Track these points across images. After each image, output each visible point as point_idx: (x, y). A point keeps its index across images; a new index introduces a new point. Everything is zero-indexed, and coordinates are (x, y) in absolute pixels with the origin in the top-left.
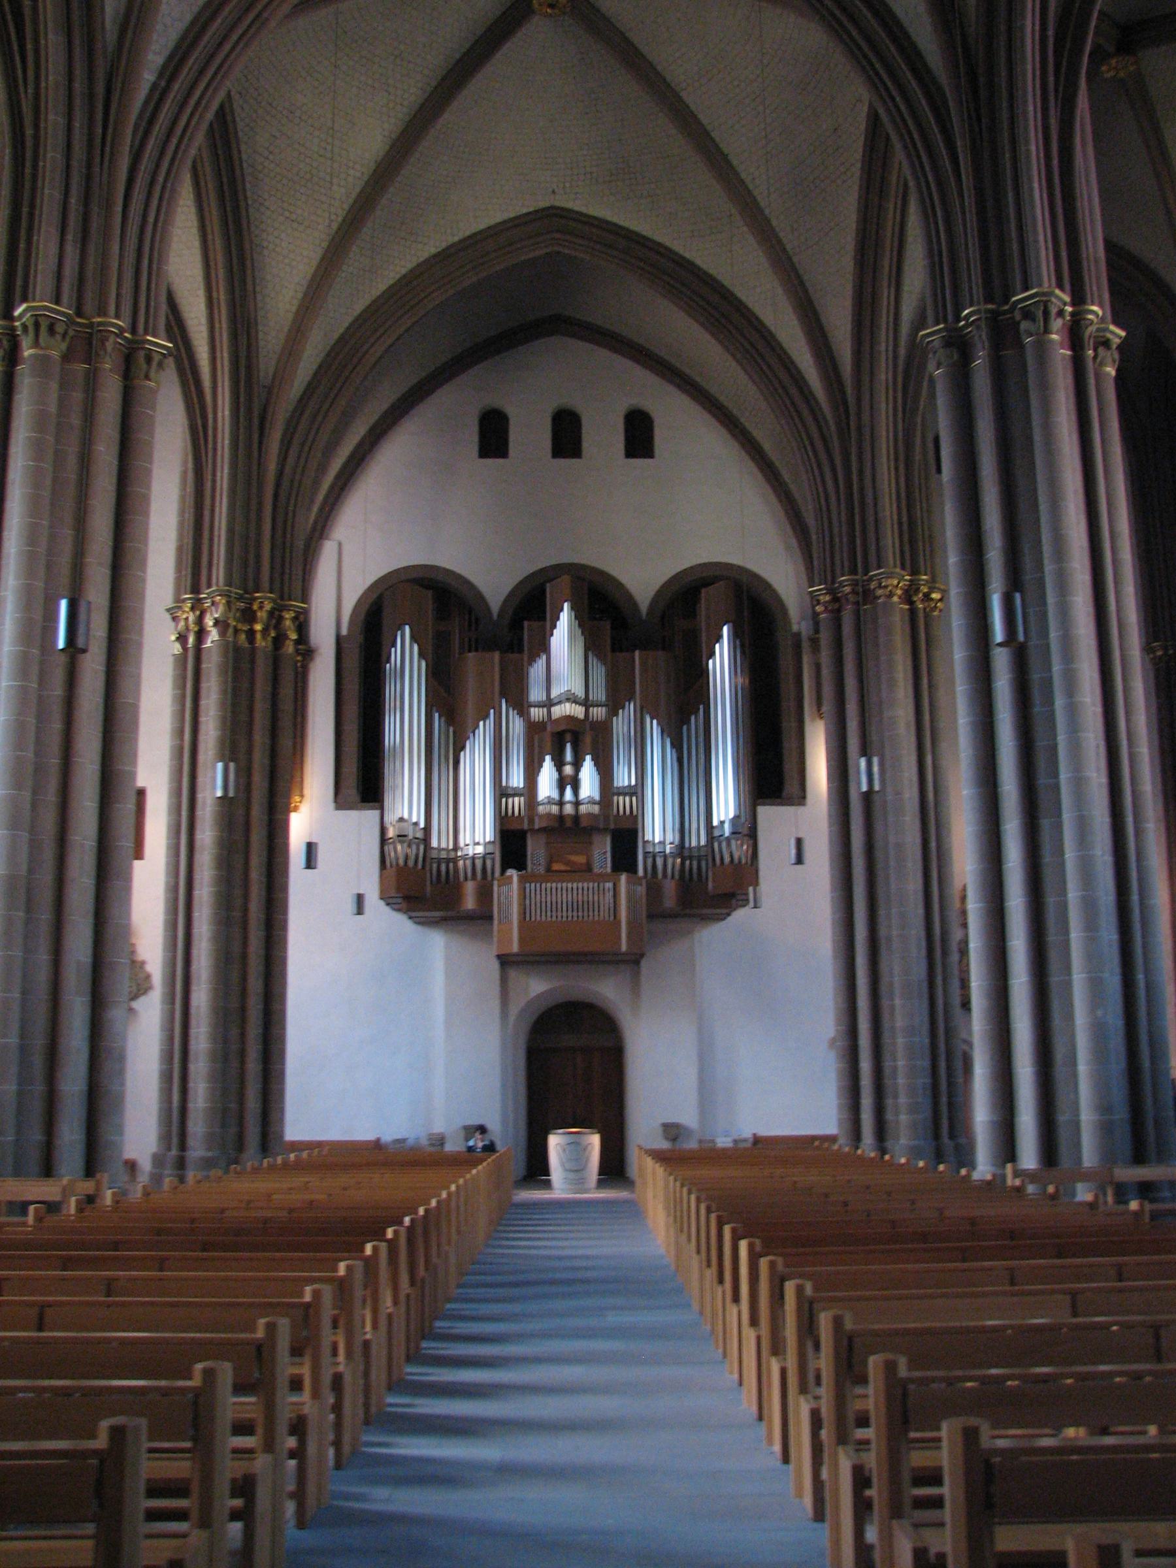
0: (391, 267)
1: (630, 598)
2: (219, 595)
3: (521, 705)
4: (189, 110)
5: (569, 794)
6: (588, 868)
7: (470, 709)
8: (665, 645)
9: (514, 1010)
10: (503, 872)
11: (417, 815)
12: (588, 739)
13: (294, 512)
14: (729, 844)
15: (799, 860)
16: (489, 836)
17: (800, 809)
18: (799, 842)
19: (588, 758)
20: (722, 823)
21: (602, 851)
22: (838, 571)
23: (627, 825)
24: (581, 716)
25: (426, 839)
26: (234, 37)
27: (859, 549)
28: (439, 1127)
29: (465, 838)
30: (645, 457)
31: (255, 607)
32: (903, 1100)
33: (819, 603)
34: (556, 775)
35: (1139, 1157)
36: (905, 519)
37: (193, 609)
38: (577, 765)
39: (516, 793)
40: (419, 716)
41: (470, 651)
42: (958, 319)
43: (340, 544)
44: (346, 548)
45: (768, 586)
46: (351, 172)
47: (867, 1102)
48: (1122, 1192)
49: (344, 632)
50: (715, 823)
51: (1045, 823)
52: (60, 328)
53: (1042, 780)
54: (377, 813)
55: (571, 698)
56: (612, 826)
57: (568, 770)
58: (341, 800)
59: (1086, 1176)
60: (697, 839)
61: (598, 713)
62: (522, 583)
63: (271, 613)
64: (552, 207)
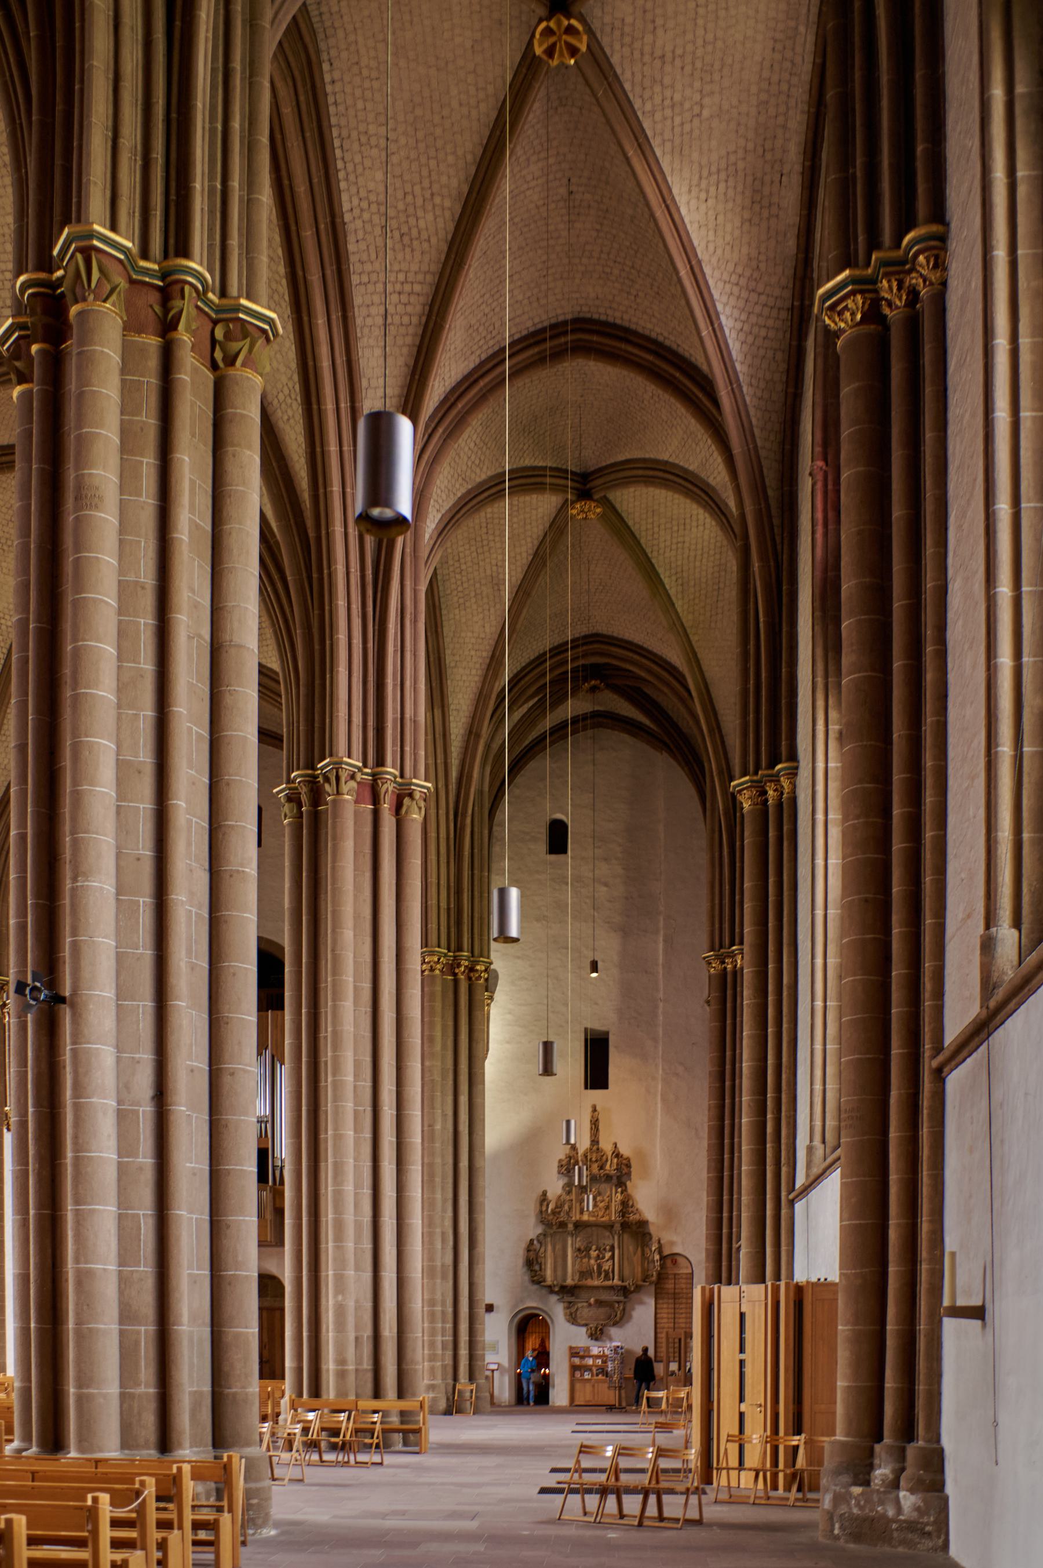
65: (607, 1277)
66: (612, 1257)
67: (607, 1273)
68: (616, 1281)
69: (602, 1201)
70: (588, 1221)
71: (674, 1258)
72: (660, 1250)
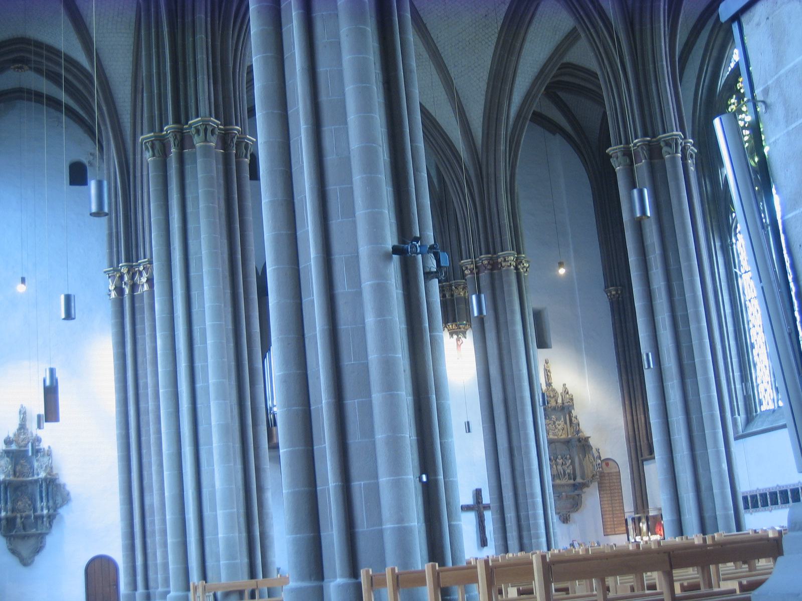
2: (148, 264)
33: (467, 268)
36: (512, 224)
37: (128, 272)
65: (570, 479)
66: (573, 463)
67: (569, 475)
68: (579, 480)
69: (559, 425)
70: (553, 439)
71: (607, 461)
72: (600, 458)
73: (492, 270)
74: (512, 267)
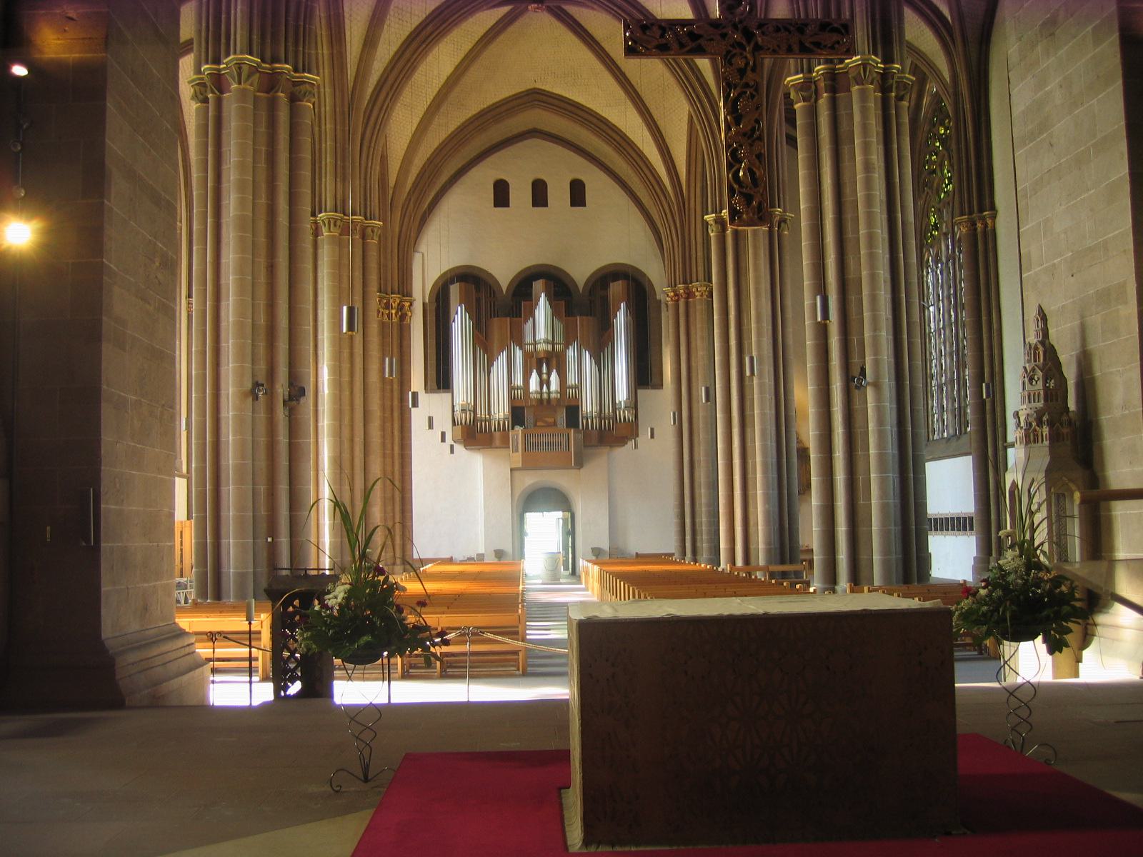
0: (453, 122)
1: (572, 280)
3: (521, 344)
4: (383, 112)
5: (545, 386)
6: (555, 424)
7: (496, 346)
8: (590, 313)
9: (518, 493)
10: (513, 429)
11: (471, 400)
12: (554, 362)
13: (407, 251)
14: (624, 412)
15: (652, 436)
16: (506, 413)
17: (661, 390)
18: (652, 430)
19: (554, 370)
20: (620, 402)
21: (561, 417)
22: (678, 282)
23: (573, 403)
24: (550, 349)
25: (475, 414)
26: (401, 76)
27: (688, 270)
28: (481, 551)
29: (494, 409)
30: (582, 206)
31: (391, 301)
32: (705, 537)
33: (668, 295)
34: (538, 379)
35: (782, 562)
38: (549, 374)
39: (518, 388)
40: (470, 354)
41: (494, 317)
42: (721, 213)
43: (423, 255)
44: (426, 255)
45: (644, 275)
46: (434, 81)
47: (688, 537)
48: (772, 575)
49: (427, 301)
50: (617, 402)
51: (749, 430)
52: (338, 223)
53: (748, 412)
54: (450, 395)
55: (546, 342)
56: (566, 404)
57: (545, 376)
58: (427, 389)
59: (760, 569)
60: (608, 410)
61: (560, 347)
62: (516, 277)
63: (399, 304)
64: (534, 89)
73: (687, 298)
74: (705, 297)
